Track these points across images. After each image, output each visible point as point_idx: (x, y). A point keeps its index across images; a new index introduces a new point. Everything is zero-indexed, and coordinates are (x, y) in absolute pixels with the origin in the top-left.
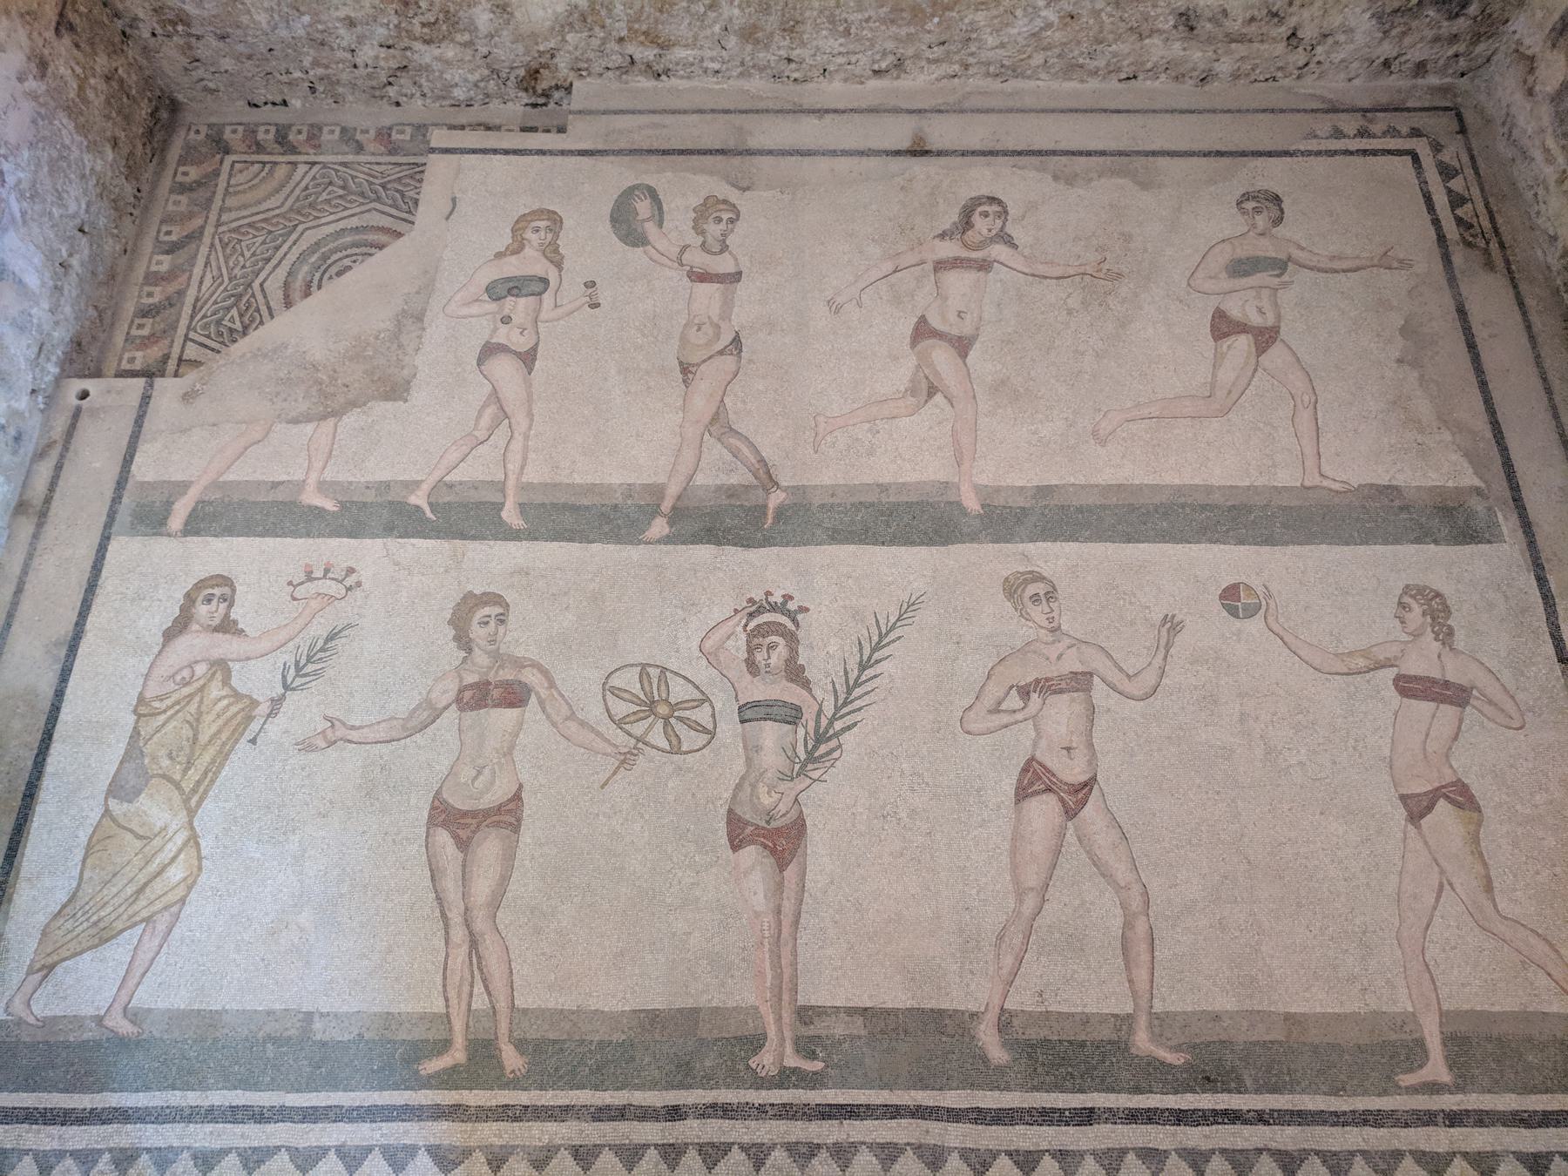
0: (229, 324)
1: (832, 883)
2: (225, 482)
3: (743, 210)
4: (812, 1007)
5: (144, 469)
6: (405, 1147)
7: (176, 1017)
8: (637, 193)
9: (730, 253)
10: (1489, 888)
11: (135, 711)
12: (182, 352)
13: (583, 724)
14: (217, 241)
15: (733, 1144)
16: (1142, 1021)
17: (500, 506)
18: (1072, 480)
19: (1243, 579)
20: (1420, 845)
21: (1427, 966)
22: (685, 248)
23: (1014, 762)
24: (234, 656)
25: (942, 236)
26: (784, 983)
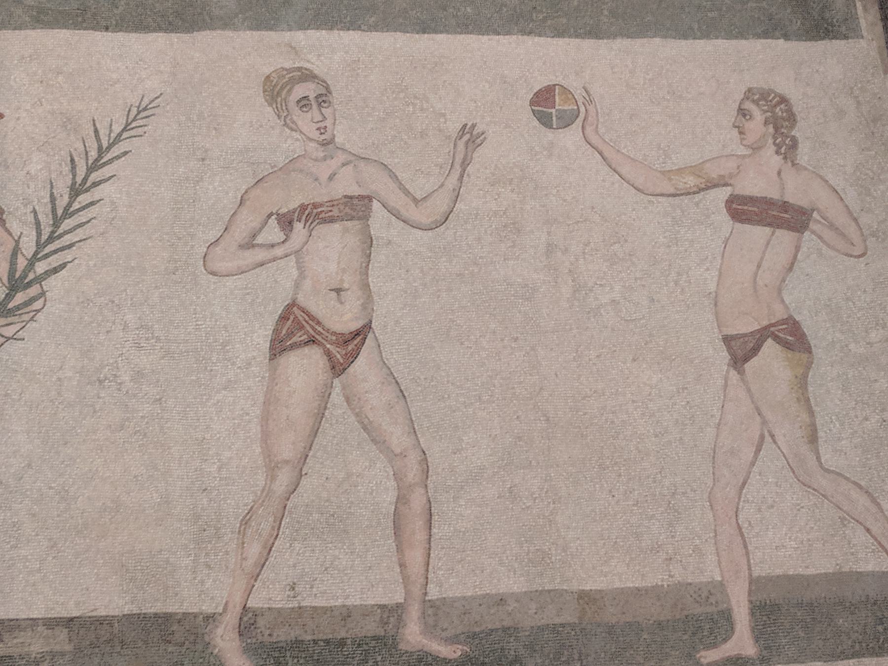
19: (560, 80)
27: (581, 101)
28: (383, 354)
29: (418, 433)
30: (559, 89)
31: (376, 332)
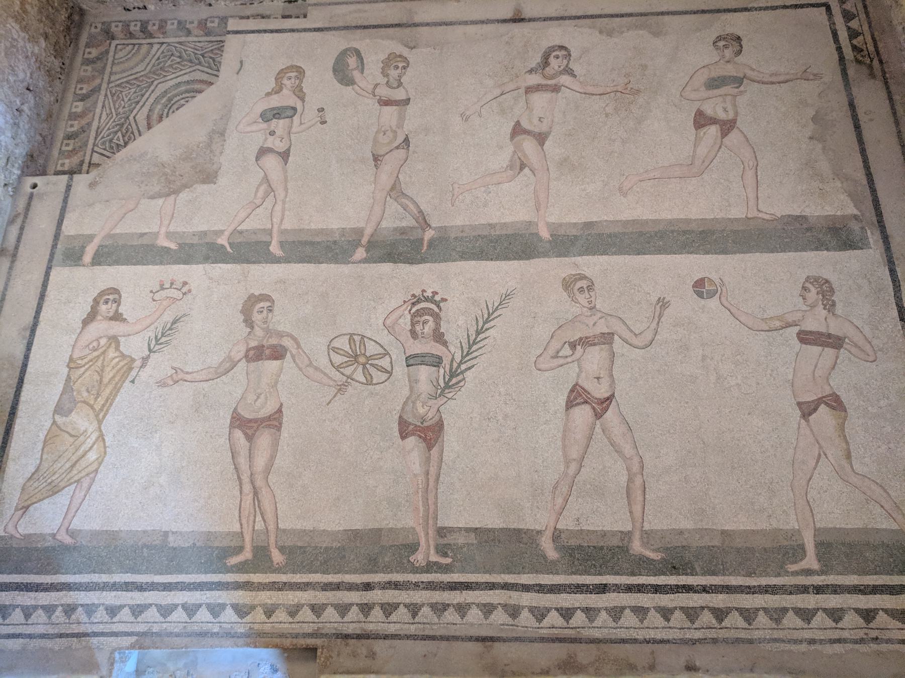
0: (117, 142)
1: (458, 457)
2: (115, 235)
3: (411, 60)
4: (445, 528)
5: (69, 228)
6: (219, 604)
7: (95, 534)
8: (349, 53)
9: (404, 88)
10: (848, 456)
11: (68, 366)
12: (91, 159)
13: (316, 369)
14: (109, 93)
15: (400, 603)
16: (637, 535)
17: (268, 244)
18: (606, 218)
19: (707, 275)
20: (808, 432)
21: (808, 502)
22: (376, 85)
23: (565, 386)
24: (121, 334)
25: (531, 71)
26: (430, 513)
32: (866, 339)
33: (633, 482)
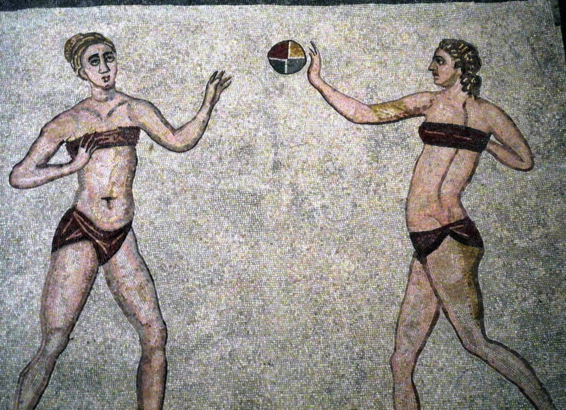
10: (479, 314)
19: (293, 37)
20: (423, 280)
21: (414, 386)
27: (308, 52)
28: (139, 247)
29: (161, 308)
30: (291, 44)
31: (135, 230)
32: (521, 136)
33: (150, 362)
